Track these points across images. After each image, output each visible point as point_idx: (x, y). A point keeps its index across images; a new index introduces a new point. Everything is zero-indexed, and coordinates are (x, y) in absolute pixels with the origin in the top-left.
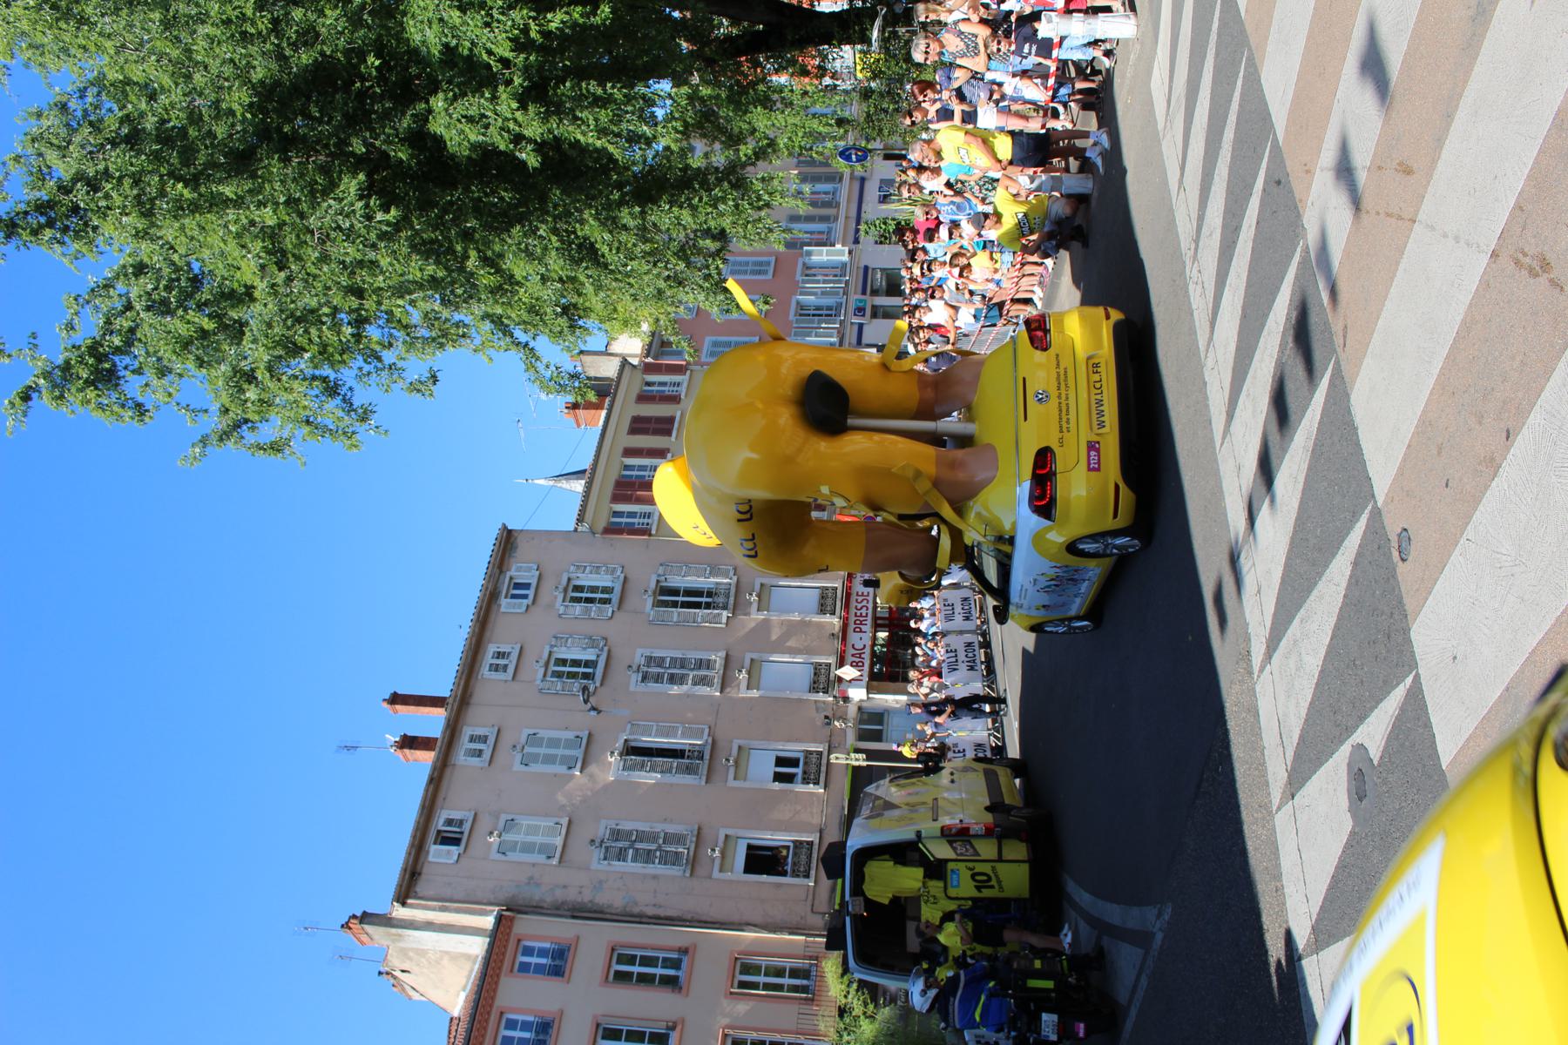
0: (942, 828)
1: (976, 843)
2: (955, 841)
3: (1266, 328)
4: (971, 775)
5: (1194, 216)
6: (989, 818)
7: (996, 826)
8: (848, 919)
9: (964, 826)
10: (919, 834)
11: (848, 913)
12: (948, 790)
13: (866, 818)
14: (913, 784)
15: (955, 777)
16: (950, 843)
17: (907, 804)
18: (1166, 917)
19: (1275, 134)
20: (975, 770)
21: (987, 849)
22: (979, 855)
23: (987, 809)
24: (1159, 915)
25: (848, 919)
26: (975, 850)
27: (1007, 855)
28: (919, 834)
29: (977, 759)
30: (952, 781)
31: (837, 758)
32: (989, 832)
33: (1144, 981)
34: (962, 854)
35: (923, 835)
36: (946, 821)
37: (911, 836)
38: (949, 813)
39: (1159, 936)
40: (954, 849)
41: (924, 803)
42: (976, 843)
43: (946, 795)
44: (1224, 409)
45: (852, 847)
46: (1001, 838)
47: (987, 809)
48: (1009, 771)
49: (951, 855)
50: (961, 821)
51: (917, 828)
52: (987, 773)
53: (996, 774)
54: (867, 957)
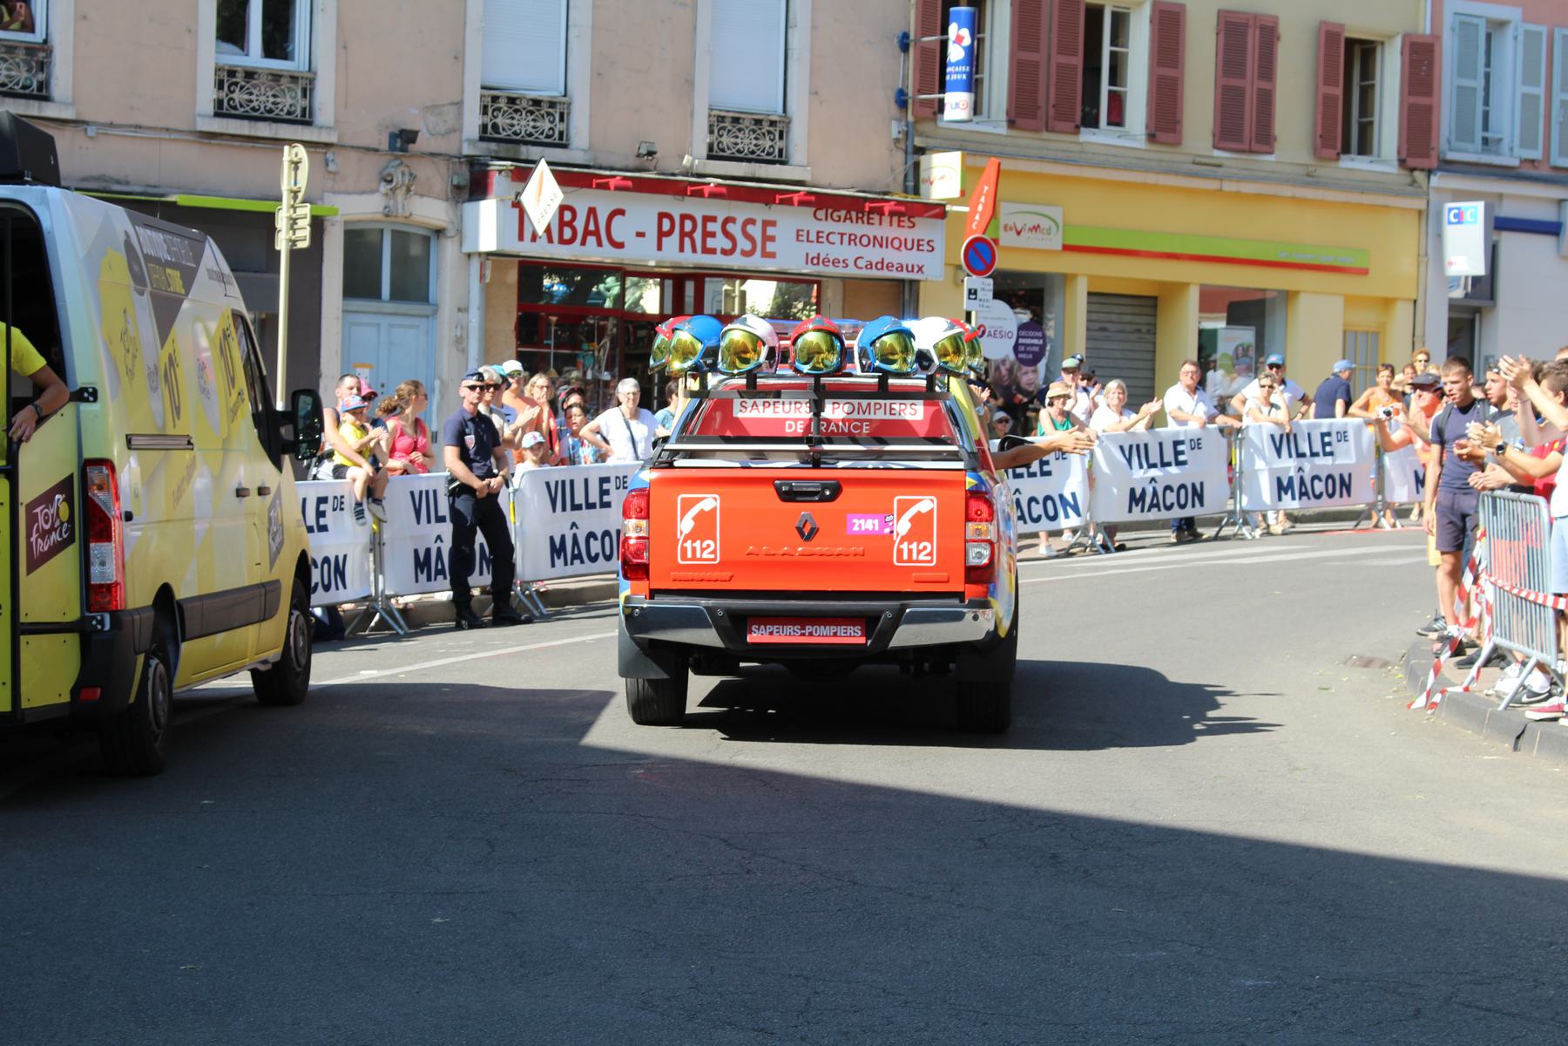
0: (107, 463)
1: (71, 553)
2: (69, 500)
4: (259, 546)
6: (138, 596)
7: (116, 616)
9: (117, 526)
10: (86, 395)
12: (217, 479)
13: (128, 244)
14: (232, 381)
15: (254, 496)
16: (65, 486)
17: (172, 362)
20: (272, 562)
22: (33, 565)
23: (165, 592)
27: (29, 644)
28: (86, 395)
29: (304, 565)
30: (241, 493)
31: (296, 165)
32: (95, 594)
35: (84, 407)
36: (130, 471)
38: (149, 479)
40: (46, 499)
41: (177, 410)
42: (71, 553)
45: (45, 201)
46: (80, 628)
47: (165, 592)
48: (274, 654)
49: (27, 494)
50: (129, 517)
51: (105, 392)
52: (268, 590)
53: (266, 615)
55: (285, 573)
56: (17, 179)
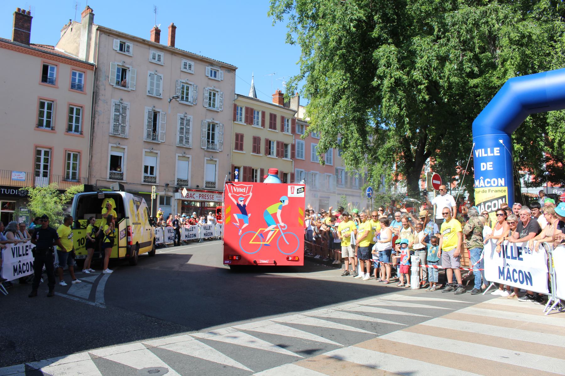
3: (313, 335)
4: (149, 236)
5: (351, 310)
6: (134, 243)
8: (96, 192)
10: (128, 218)
11: (98, 193)
12: (144, 228)
16: (125, 229)
18: (101, 306)
19: (380, 336)
20: (151, 238)
21: (123, 242)
22: (121, 239)
23: (137, 242)
24: (101, 304)
25: (96, 192)
26: (122, 238)
28: (128, 218)
30: (147, 230)
32: (129, 243)
33: (76, 299)
34: (121, 233)
36: (133, 228)
37: (127, 216)
38: (135, 228)
39: (94, 304)
40: (122, 231)
41: (139, 220)
42: (126, 237)
43: (142, 228)
44: (284, 321)
47: (137, 242)
48: (151, 250)
49: (120, 230)
52: (150, 242)
53: (150, 245)
54: (82, 200)
55: (152, 240)
56: (119, 191)
